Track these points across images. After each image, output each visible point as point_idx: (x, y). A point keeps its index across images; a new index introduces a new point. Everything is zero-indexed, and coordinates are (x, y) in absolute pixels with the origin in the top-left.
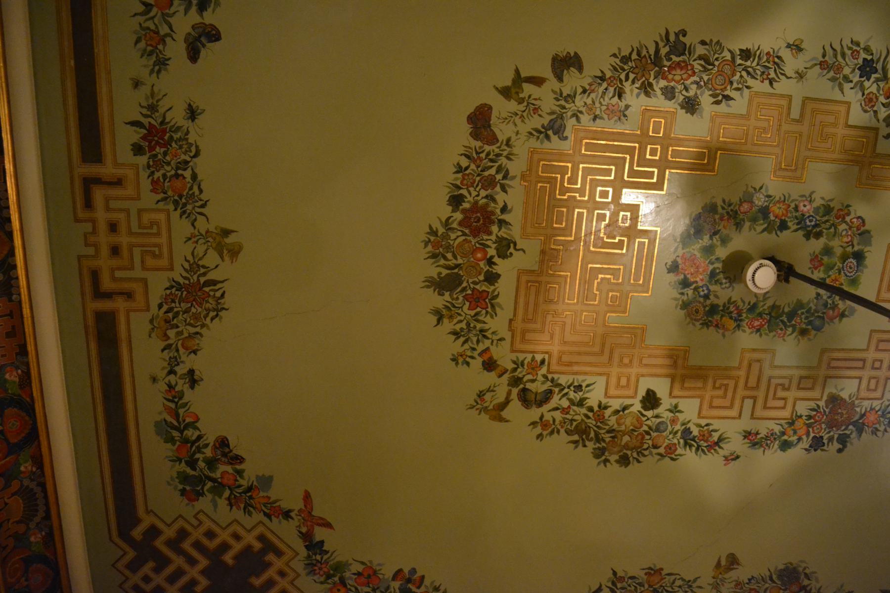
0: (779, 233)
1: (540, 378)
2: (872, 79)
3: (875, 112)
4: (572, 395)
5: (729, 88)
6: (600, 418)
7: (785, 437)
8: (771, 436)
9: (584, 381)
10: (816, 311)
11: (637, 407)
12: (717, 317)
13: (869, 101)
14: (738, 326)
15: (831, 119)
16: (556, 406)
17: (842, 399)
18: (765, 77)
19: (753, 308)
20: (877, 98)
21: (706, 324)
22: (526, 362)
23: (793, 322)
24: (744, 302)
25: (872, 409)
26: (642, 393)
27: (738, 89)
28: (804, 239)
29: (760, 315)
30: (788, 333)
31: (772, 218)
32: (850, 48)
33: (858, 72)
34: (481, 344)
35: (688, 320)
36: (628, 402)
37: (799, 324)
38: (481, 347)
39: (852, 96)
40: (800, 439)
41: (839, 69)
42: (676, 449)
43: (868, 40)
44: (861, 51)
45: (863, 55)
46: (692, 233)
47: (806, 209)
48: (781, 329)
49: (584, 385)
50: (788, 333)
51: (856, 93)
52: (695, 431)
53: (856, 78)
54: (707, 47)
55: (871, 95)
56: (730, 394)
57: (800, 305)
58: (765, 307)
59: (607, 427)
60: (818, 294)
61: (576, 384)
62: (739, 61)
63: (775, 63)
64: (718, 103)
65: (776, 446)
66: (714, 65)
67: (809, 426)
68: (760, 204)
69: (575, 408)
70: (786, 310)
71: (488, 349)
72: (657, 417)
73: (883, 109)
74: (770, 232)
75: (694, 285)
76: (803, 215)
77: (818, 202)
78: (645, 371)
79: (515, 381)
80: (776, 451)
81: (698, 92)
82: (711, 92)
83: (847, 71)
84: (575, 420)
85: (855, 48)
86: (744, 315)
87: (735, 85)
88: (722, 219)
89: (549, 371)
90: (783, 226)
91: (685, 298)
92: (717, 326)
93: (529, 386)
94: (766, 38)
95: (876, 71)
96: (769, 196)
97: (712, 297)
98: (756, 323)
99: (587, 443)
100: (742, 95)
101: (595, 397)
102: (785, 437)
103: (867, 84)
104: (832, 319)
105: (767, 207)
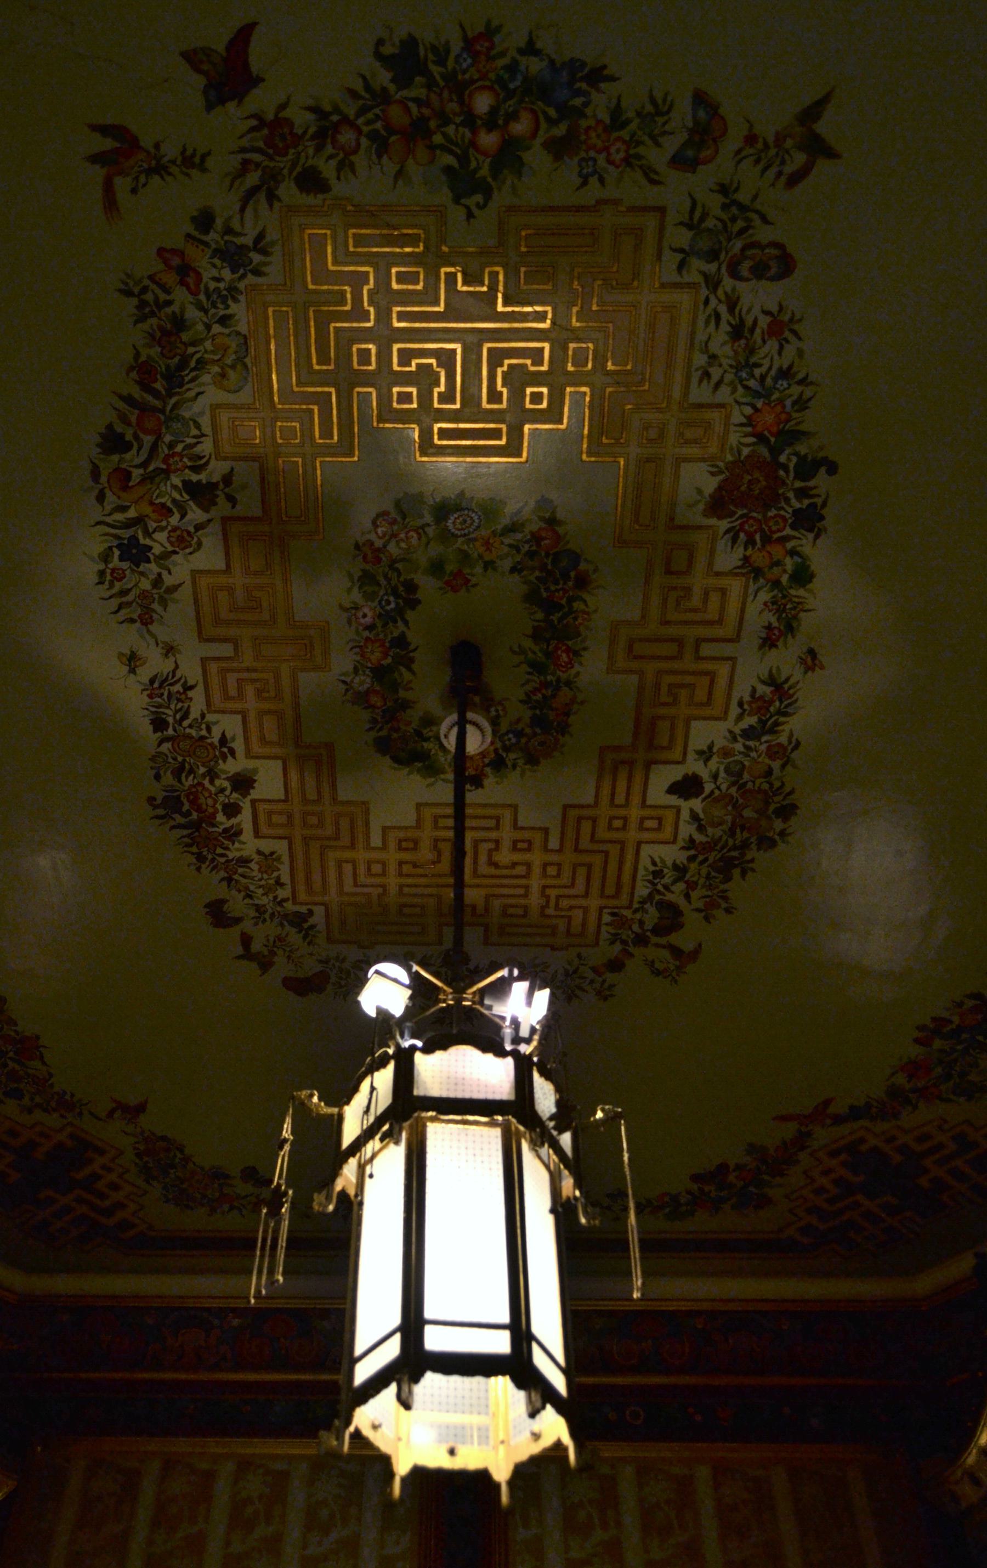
0: (412, 647)
1: (638, 916)
2: (148, 542)
3: (198, 527)
4: (667, 880)
5: (209, 741)
6: (709, 847)
7: (785, 579)
8: (777, 606)
9: (646, 869)
10: (543, 568)
11: (696, 804)
12: (552, 715)
13: (184, 541)
14: (568, 683)
15: (223, 597)
16: (682, 897)
17: (720, 488)
18: (183, 697)
19: (537, 667)
20: (175, 529)
21: (564, 729)
22: (613, 931)
23: (564, 602)
24: (528, 681)
25: (750, 421)
26: (674, 800)
27: (209, 729)
28: (419, 608)
29: (548, 654)
30: (582, 607)
31: (389, 660)
32: (112, 585)
33: (143, 567)
34: (586, 975)
35: (555, 754)
36: (685, 815)
37: (565, 591)
38: (590, 975)
39: (181, 569)
40: (793, 553)
41: (144, 595)
42: (779, 745)
43: (92, 559)
44: (111, 566)
45: (115, 562)
46: (420, 765)
47: (369, 613)
48: (575, 619)
49: (652, 868)
50: (582, 607)
51: (175, 564)
52: (752, 720)
53: (153, 568)
54: (162, 773)
55: (173, 539)
56: (689, 679)
57: (532, 597)
58: (536, 649)
59: (725, 838)
60: (513, 570)
61: (651, 877)
62: (170, 732)
63: (160, 687)
64: (232, 752)
65: (801, 592)
66: (184, 760)
67: (767, 540)
68: (368, 680)
69: (688, 876)
70: (540, 615)
71: (595, 970)
72: (715, 777)
73: (190, 516)
74: (412, 660)
75: (500, 751)
76: (380, 616)
77: (356, 596)
78: (636, 800)
79: (641, 940)
80: (811, 591)
81: (224, 776)
82: (220, 761)
83: (146, 584)
84: (709, 873)
85: (109, 578)
86: (549, 678)
87: (204, 733)
88: (397, 730)
89: (629, 907)
90: (401, 642)
91: (520, 762)
92: (567, 714)
93: (649, 925)
94: (132, 701)
95: (134, 538)
96: (356, 670)
97: (520, 727)
98: (564, 657)
99: (748, 857)
100: (216, 723)
101: (671, 854)
102: (785, 579)
103: (157, 550)
104: (558, 538)
105: (372, 670)
